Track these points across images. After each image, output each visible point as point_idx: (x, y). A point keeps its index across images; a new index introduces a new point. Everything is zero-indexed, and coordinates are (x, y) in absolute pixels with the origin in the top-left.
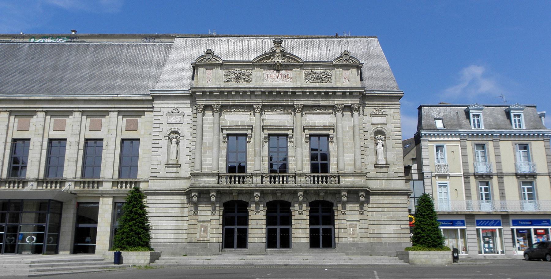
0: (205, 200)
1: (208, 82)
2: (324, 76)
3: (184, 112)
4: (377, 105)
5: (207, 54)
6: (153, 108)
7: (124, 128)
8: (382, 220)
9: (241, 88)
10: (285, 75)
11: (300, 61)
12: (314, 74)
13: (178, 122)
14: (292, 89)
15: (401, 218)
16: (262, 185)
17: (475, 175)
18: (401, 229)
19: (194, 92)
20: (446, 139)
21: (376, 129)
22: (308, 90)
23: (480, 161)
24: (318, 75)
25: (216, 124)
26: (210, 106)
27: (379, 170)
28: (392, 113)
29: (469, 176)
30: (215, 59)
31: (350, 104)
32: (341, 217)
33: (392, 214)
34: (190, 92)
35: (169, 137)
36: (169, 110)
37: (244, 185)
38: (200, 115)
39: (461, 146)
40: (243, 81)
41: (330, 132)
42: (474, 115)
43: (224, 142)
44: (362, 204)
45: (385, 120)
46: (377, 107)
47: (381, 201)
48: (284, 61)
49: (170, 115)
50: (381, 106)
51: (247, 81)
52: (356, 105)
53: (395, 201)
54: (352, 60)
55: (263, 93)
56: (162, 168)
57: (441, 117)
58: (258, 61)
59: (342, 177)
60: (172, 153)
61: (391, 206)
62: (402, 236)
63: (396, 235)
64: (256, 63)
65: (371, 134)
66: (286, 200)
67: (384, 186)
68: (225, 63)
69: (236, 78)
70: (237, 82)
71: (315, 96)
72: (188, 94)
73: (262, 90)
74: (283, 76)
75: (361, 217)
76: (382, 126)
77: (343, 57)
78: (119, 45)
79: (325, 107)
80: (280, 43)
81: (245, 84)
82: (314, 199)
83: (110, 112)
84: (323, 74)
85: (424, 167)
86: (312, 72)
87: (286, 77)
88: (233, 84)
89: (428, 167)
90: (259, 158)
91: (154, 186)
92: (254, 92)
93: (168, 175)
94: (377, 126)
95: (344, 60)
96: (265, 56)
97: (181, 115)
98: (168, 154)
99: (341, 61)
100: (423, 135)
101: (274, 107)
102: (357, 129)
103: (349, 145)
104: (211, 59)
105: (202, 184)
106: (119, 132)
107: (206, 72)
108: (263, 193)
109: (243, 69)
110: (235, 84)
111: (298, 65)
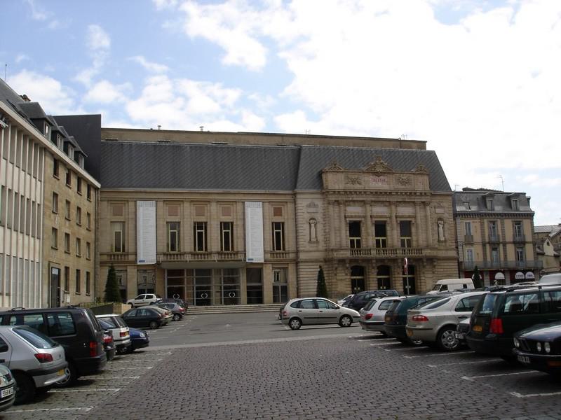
17: (489, 243)
27: (441, 244)
47: (442, 264)
49: (309, 206)
56: (306, 244)
71: (403, 195)
93: (311, 249)
105: (341, 256)
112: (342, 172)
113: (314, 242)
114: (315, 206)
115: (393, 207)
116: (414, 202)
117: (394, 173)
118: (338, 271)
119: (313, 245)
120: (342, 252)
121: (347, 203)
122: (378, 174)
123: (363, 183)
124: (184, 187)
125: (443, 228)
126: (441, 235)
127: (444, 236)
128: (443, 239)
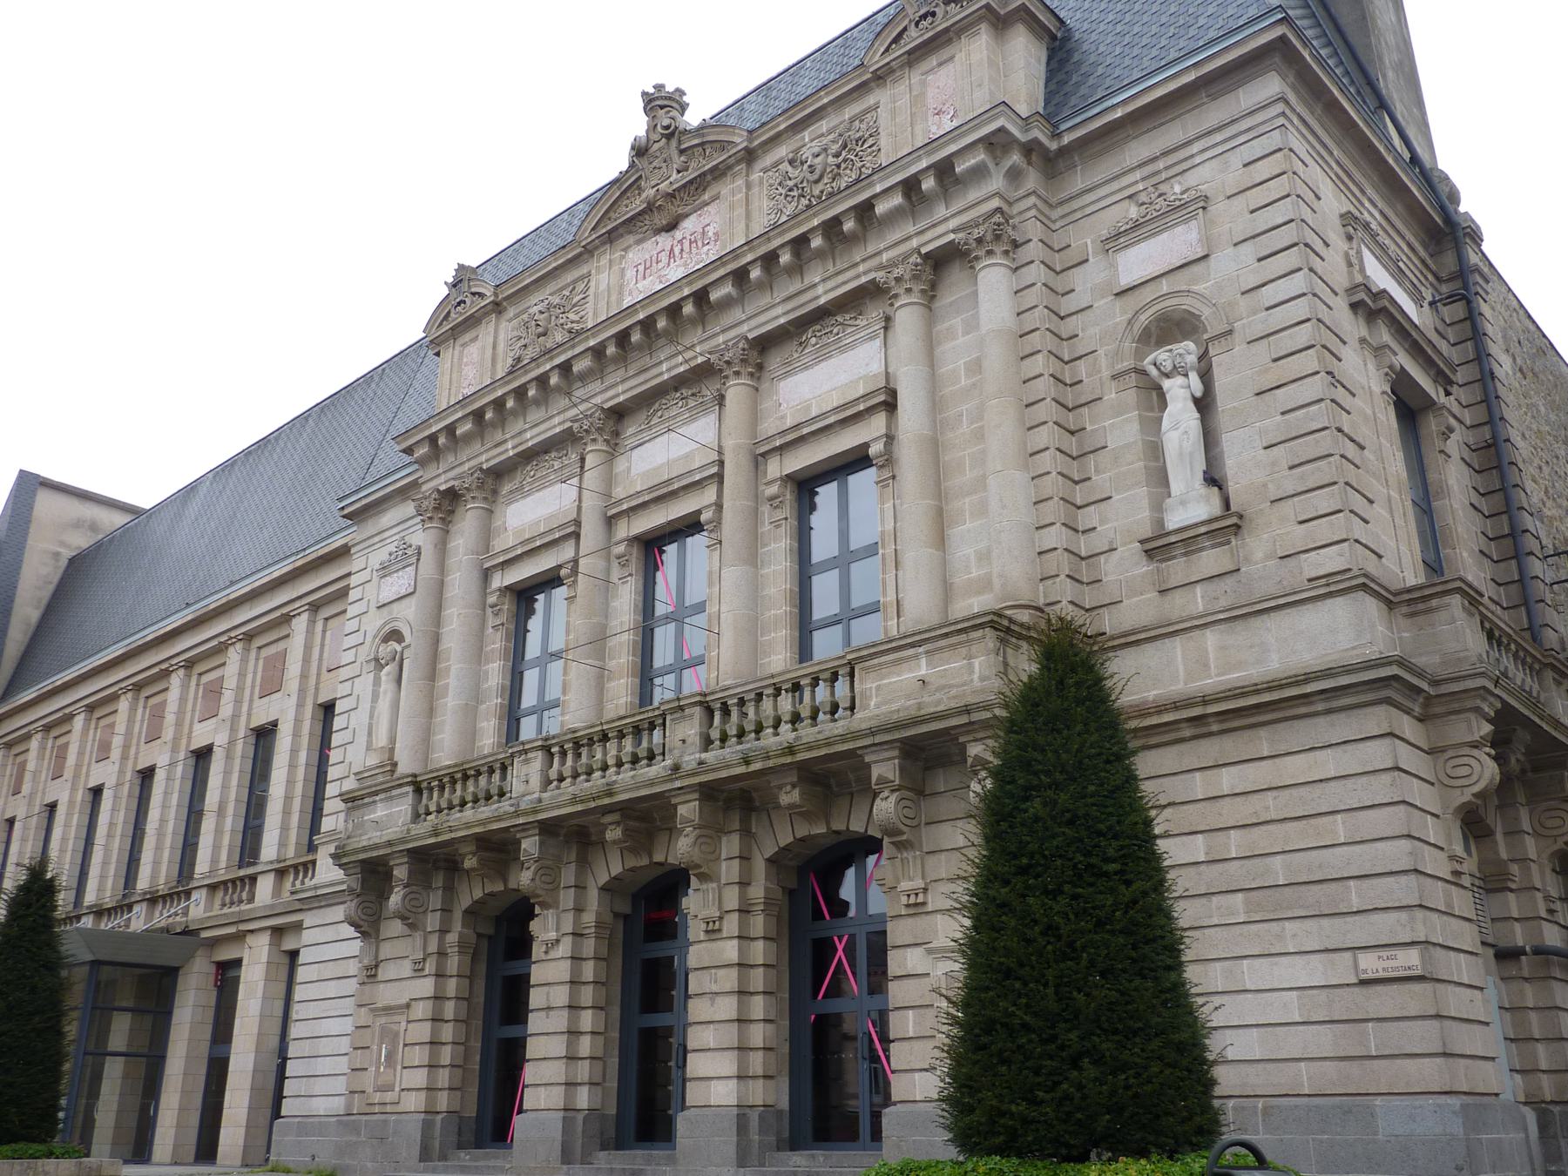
4: (1138, 175)
8: (1215, 921)
14: (690, 283)
15: (1355, 896)
18: (1364, 983)
27: (1178, 570)
33: (1278, 869)
50: (1161, 164)
53: (1295, 768)
61: (1272, 806)
62: (1374, 1039)
63: (1323, 1040)
67: (1213, 671)
76: (1180, 282)
82: (785, 838)
84: (835, 148)
94: (1148, 294)
111: (732, 160)
118: (386, 950)
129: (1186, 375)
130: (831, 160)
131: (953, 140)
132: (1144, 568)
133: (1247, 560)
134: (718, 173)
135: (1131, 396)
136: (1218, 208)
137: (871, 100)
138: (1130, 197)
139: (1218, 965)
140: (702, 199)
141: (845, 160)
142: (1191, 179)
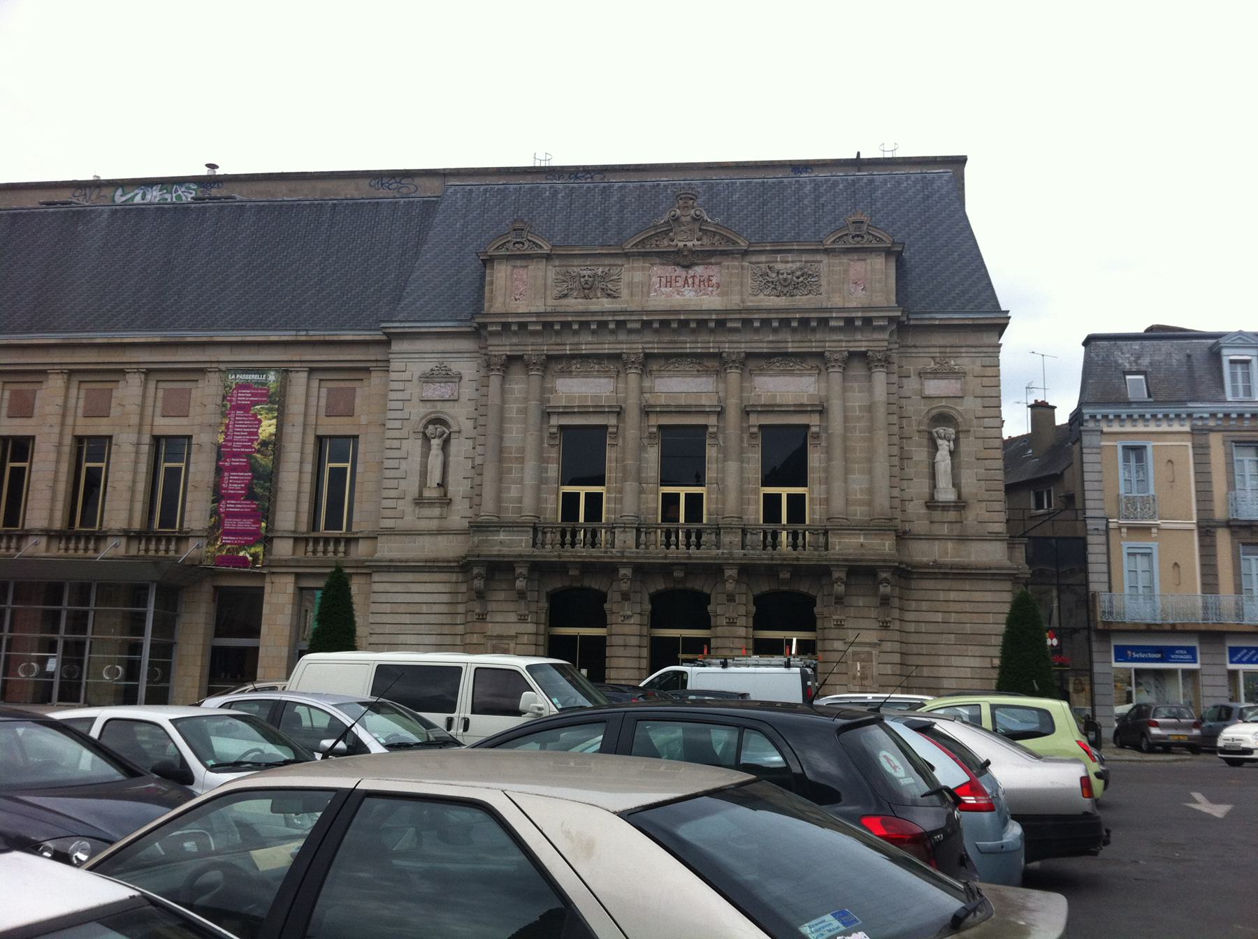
0: (504, 586)
1: (516, 300)
2: (801, 279)
3: (462, 371)
4: (938, 350)
5: (514, 230)
6: (388, 361)
7: (322, 411)
9: (594, 313)
10: (702, 279)
11: (739, 241)
12: (774, 275)
13: (447, 397)
16: (638, 553)
19: (484, 326)
20: (1152, 428)
21: (934, 412)
22: (756, 316)
23: (1248, 489)
24: (785, 276)
25: (533, 404)
26: (520, 358)
27: (938, 515)
28: (977, 369)
29: (1212, 530)
30: (534, 243)
31: (863, 349)
32: (833, 633)
34: (475, 325)
35: (424, 434)
36: (427, 367)
37: (594, 552)
38: (495, 381)
39: (1193, 447)
40: (599, 295)
41: (814, 420)
42: (1232, 362)
43: (552, 446)
44: (885, 601)
45: (959, 386)
46: (938, 355)
47: (942, 596)
48: (700, 242)
49: (428, 378)
50: (948, 350)
51: (609, 295)
52: (879, 351)
53: (978, 596)
54: (873, 236)
55: (647, 324)
56: (406, 506)
57: (1143, 368)
58: (636, 245)
59: (835, 534)
60: (431, 472)
61: (968, 607)
64: (632, 250)
65: (920, 423)
66: (697, 587)
68: (557, 253)
69: (584, 289)
70: (586, 297)
71: (775, 331)
72: (469, 329)
73: (645, 318)
74: (697, 281)
75: (883, 634)
76: (950, 403)
77: (851, 229)
78: (314, 204)
79: (802, 356)
80: (691, 199)
81: (606, 304)
83: (291, 371)
84: (799, 273)
85: (1089, 504)
86: (770, 268)
87: (706, 284)
88: (575, 304)
89: (1098, 504)
90: (635, 485)
91: (388, 550)
92: (624, 322)
93: (423, 525)
94: (936, 403)
95: (853, 237)
96: (653, 232)
97: (453, 380)
98: (424, 474)
99: (845, 237)
100: (1087, 417)
101: (674, 360)
102: (881, 412)
103: (860, 453)
104: (523, 244)
106: (312, 420)
107: (512, 274)
108: (642, 571)
109: (602, 265)
110: (581, 304)
112: (548, 257)
113: (431, 503)
114: (448, 377)
115: (734, 375)
116: (820, 355)
117: (745, 253)
118: (492, 606)
119: (427, 512)
120: (502, 536)
121: (552, 363)
122: (684, 259)
123: (625, 293)
124: (54, 330)
125: (952, 453)
126: (944, 481)
127: (956, 485)
128: (946, 494)
129: (949, 441)
130: (795, 278)
131: (876, 311)
132: (924, 511)
133: (966, 519)
134: (724, 253)
135: (925, 442)
136: (969, 378)
137: (818, 257)
138: (932, 357)
139: (943, 657)
140: (710, 261)
141: (802, 282)
142: (959, 361)
